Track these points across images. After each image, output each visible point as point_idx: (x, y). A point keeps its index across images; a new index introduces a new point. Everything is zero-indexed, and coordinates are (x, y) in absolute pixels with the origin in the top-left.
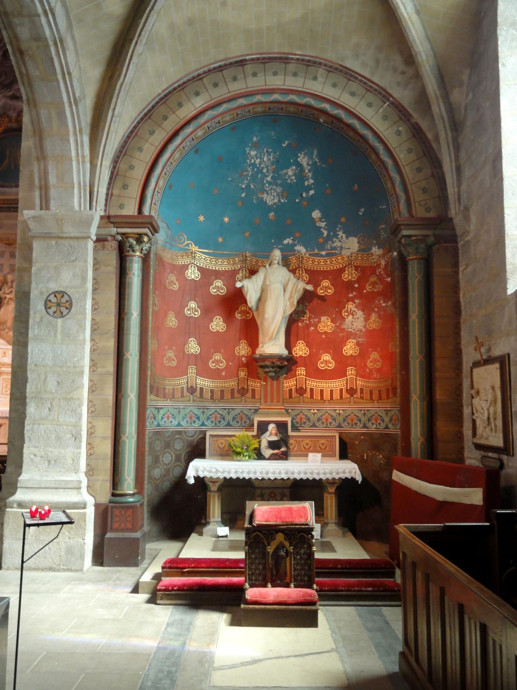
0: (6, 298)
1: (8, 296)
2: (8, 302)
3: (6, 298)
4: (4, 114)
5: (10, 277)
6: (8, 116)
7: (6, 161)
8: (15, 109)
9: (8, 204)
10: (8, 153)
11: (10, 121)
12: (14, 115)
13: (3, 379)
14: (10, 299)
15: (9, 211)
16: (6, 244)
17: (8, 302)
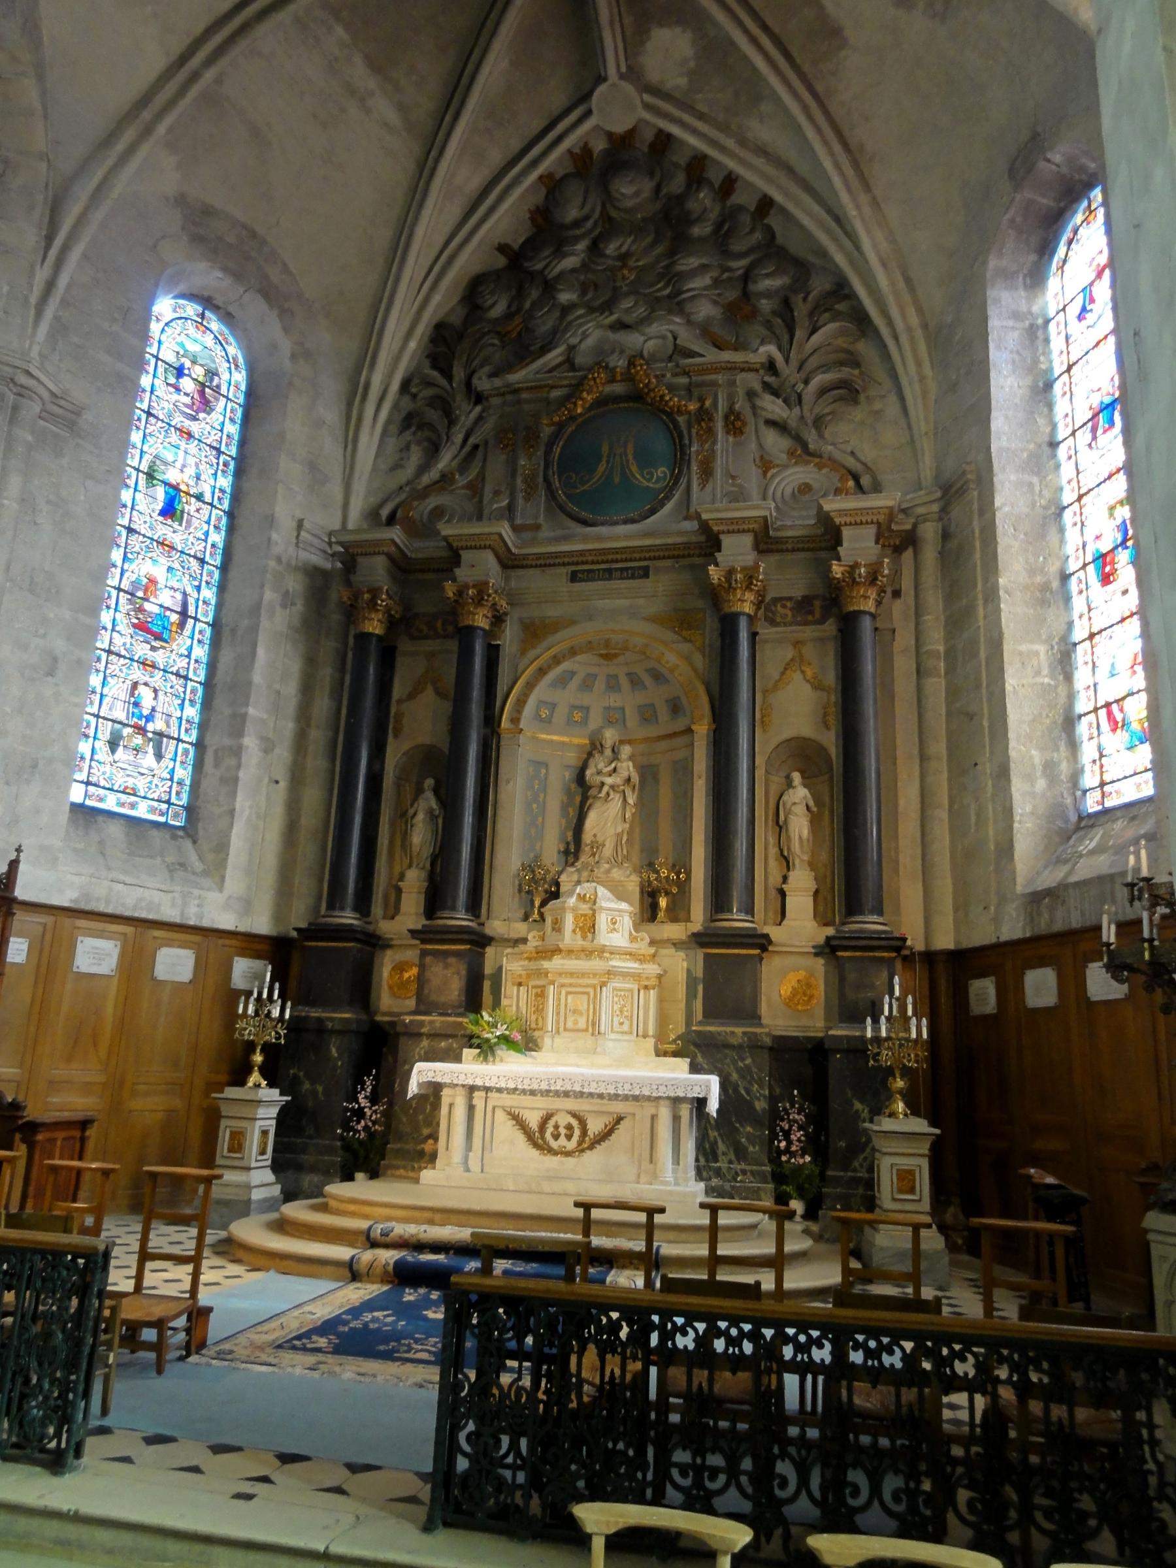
0: (603, 784)
1: (609, 781)
2: (608, 794)
3: (603, 784)
4: (599, 363)
5: (610, 736)
6: (607, 367)
7: (602, 468)
8: (622, 352)
9: (607, 562)
10: (605, 448)
11: (612, 380)
12: (619, 364)
13: (614, 989)
14: (612, 787)
15: (610, 579)
16: (601, 656)
17: (608, 794)
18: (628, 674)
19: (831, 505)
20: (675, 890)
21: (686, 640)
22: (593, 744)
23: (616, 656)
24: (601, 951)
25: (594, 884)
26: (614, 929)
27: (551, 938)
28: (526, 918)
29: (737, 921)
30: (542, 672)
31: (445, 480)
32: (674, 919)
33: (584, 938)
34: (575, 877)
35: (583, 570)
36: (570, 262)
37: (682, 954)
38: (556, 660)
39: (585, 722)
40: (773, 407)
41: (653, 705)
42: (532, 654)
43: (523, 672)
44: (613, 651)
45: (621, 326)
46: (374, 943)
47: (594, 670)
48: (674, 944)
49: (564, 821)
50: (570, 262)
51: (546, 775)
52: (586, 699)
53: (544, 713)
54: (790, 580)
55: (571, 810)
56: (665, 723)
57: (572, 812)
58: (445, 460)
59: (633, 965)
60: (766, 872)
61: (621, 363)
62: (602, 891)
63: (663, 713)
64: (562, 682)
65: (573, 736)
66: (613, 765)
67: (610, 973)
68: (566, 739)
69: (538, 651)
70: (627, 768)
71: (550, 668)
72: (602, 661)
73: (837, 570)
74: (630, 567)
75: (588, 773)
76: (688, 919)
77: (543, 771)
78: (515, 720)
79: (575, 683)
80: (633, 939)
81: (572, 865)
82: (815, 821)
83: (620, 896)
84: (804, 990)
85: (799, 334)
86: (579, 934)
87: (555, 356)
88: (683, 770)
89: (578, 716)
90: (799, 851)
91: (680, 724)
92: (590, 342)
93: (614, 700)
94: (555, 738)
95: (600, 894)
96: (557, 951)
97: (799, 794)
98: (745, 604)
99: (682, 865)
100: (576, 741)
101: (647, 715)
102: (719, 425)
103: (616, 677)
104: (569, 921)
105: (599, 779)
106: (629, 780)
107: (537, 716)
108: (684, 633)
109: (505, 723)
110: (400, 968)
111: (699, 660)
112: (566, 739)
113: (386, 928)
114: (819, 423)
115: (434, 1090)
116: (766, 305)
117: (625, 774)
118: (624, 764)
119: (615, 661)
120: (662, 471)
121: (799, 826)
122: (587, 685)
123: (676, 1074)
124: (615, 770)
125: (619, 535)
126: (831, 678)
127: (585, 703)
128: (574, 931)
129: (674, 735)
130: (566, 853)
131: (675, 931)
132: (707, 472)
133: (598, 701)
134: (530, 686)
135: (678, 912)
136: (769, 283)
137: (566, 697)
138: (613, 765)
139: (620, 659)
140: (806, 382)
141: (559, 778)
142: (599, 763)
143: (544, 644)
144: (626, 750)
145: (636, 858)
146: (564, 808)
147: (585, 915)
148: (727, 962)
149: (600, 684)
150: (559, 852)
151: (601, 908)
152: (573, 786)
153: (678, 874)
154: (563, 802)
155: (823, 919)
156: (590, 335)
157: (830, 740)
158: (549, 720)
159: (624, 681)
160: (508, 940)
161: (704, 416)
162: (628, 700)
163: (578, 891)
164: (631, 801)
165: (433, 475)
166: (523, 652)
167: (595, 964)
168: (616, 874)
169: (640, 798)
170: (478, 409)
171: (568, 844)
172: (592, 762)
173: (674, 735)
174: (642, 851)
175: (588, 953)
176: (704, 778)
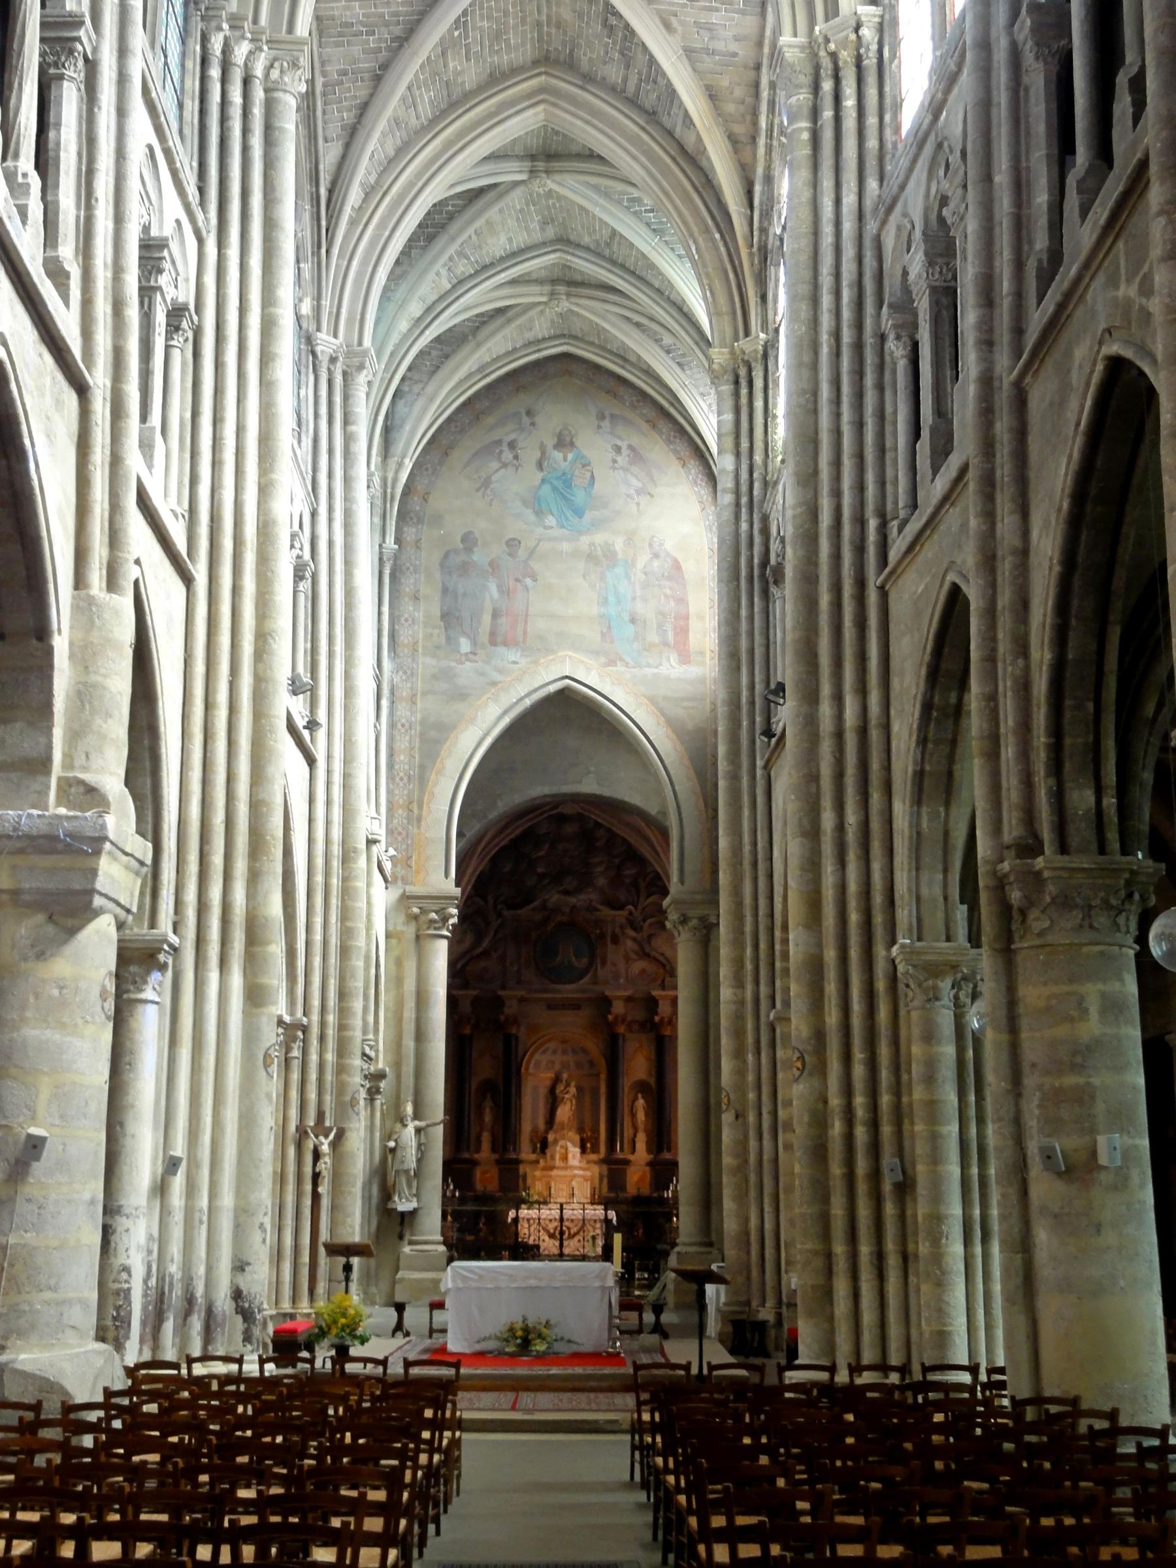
5: (565, 1076)
19: (655, 993)
24: (572, 1168)
28: (534, 1152)
29: (619, 1155)
31: (485, 954)
35: (552, 1006)
36: (542, 853)
40: (632, 933)
45: (567, 893)
46: (474, 1163)
50: (542, 853)
54: (639, 1015)
58: (485, 944)
59: (581, 1172)
60: (628, 1132)
61: (568, 910)
62: (569, 1144)
64: (544, 1052)
67: (575, 1176)
70: (573, 1090)
73: (657, 1019)
74: (575, 1006)
75: (558, 1091)
78: (527, 1069)
82: (646, 1115)
83: (575, 1146)
84: (642, 1179)
85: (641, 899)
87: (536, 904)
88: (595, 1092)
90: (641, 1126)
92: (554, 899)
96: (552, 1168)
97: (641, 1102)
98: (621, 1029)
99: (596, 1130)
101: (579, 1065)
102: (609, 939)
104: (557, 1157)
109: (523, 1070)
110: (483, 1173)
113: (476, 1156)
114: (650, 937)
115: (516, 1220)
116: (627, 881)
120: (585, 960)
121: (641, 1116)
122: (554, 1052)
123: (599, 1212)
125: (568, 991)
126: (653, 1056)
131: (594, 1157)
132: (604, 962)
134: (533, 1054)
135: (595, 1150)
136: (630, 872)
140: (644, 921)
141: (543, 1091)
142: (560, 1088)
144: (573, 1084)
148: (615, 1170)
155: (649, 1151)
156: (554, 898)
157: (652, 1081)
161: (602, 936)
162: (570, 1058)
165: (480, 950)
167: (568, 1173)
170: (500, 920)
175: (566, 1168)
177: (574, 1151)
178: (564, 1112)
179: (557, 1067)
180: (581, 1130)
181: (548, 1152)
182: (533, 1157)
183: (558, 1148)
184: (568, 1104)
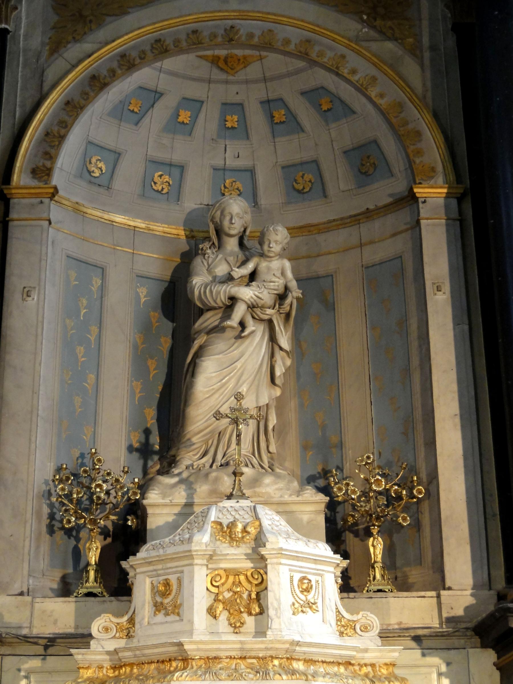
0: (233, 299)
1: (247, 293)
2: (242, 324)
3: (233, 299)
5: (237, 211)
14: (252, 307)
16: (215, 61)
17: (242, 324)
18: (267, 103)
20: (405, 520)
21: (385, 35)
22: (191, 237)
23: (245, 62)
25: (245, 503)
26: (310, 605)
27: (153, 630)
28: (65, 590)
30: (97, 83)
32: (403, 585)
33: (236, 627)
34: (180, 496)
37: (436, 661)
38: (127, 63)
39: (176, 193)
41: (316, 162)
42: (73, 51)
43: (54, 86)
44: (239, 52)
47: (196, 91)
48: (417, 639)
49: (138, 386)
51: (103, 288)
52: (180, 150)
53: (99, 167)
55: (152, 364)
56: (343, 195)
57: (157, 371)
62: (269, 518)
63: (338, 176)
65: (155, 220)
66: (250, 266)
68: (140, 224)
69: (87, 47)
70: (278, 271)
71: (113, 75)
72: (217, 74)
75: (198, 281)
76: (438, 582)
77: (97, 282)
78: (42, 172)
79: (160, 113)
80: (345, 628)
81: (165, 471)
86: (223, 616)
89: (162, 181)
91: (382, 192)
93: (235, 154)
94: (119, 218)
95: (266, 523)
100: (159, 228)
101: (303, 182)
103: (239, 107)
105: (223, 292)
106: (281, 297)
107: (84, 171)
108: (378, 22)
111: (412, 70)
112: (140, 224)
117: (278, 284)
118: (276, 264)
119: (241, 76)
124: (253, 276)
127: (177, 157)
128: (211, 611)
129: (368, 215)
130: (144, 451)
131: (416, 609)
133: (201, 156)
134: (73, 108)
135: (414, 564)
137: (142, 142)
138: (250, 266)
139: (253, 71)
141: (127, 300)
143: (101, 34)
144: (278, 237)
145: (292, 461)
146: (140, 358)
147: (237, 573)
149: (208, 121)
150: (131, 449)
151: (281, 553)
152: (156, 315)
153: (406, 483)
154: (135, 347)
158: (104, 184)
159: (257, 118)
160: (26, 639)
162: (264, 155)
163: (213, 515)
164: (284, 341)
166: (56, 47)
168: (270, 486)
169: (296, 339)
171: (147, 432)
172: (198, 263)
173: (368, 215)
174: (305, 448)
176: (447, 287)
177: (302, 560)
178: (233, 376)
179: (196, 195)
180: (321, 480)
181: (142, 570)
182: (59, 614)
183: (203, 539)
184: (257, 332)
